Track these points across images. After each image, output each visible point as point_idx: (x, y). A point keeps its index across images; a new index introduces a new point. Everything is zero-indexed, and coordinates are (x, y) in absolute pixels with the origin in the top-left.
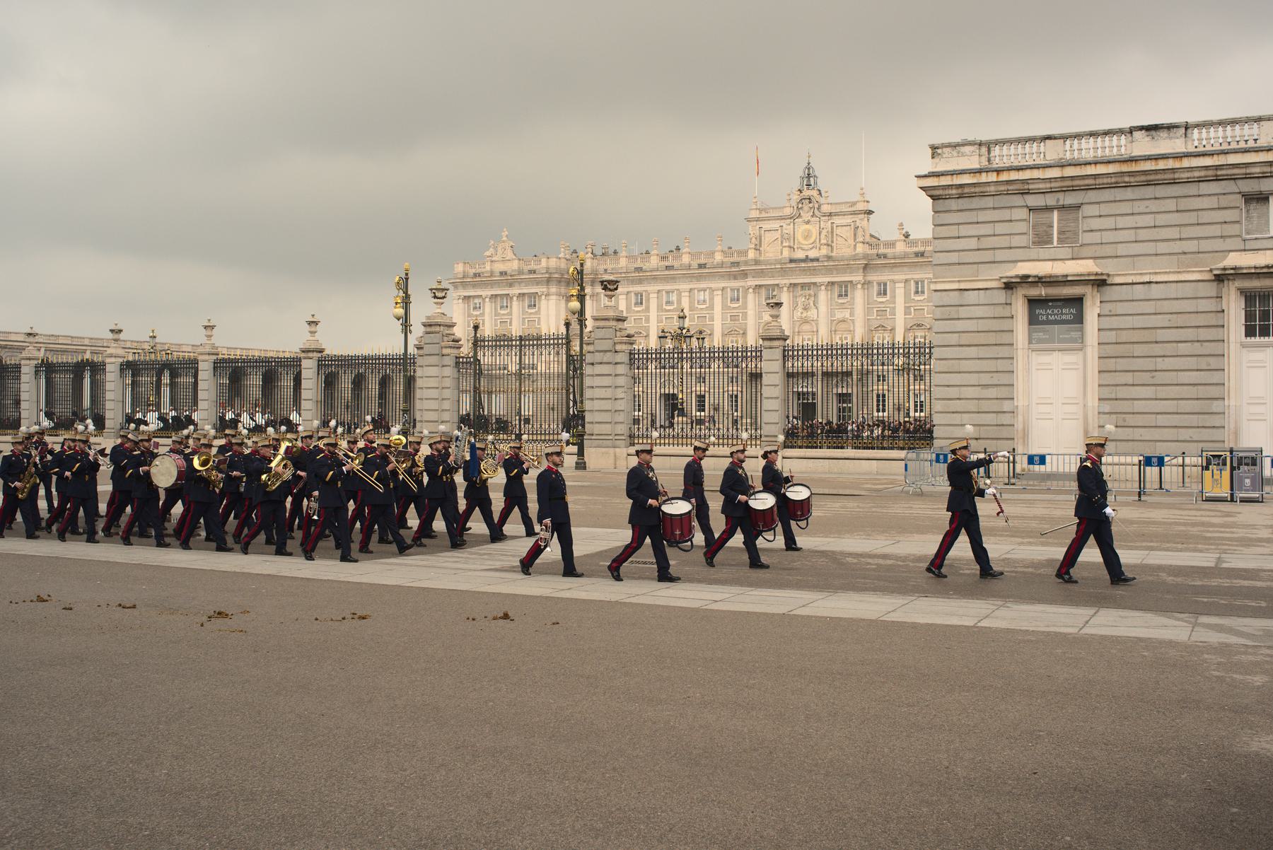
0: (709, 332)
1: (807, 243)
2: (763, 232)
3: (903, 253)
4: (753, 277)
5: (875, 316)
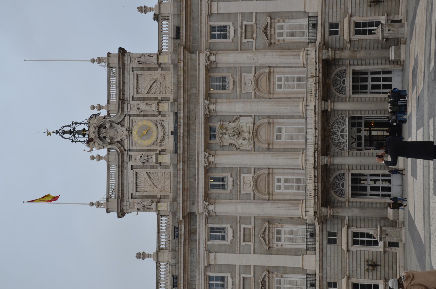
0: (266, 273)
1: (155, 133)
2: (138, 194)
3: (176, 4)
4: (194, 204)
5: (251, 40)
